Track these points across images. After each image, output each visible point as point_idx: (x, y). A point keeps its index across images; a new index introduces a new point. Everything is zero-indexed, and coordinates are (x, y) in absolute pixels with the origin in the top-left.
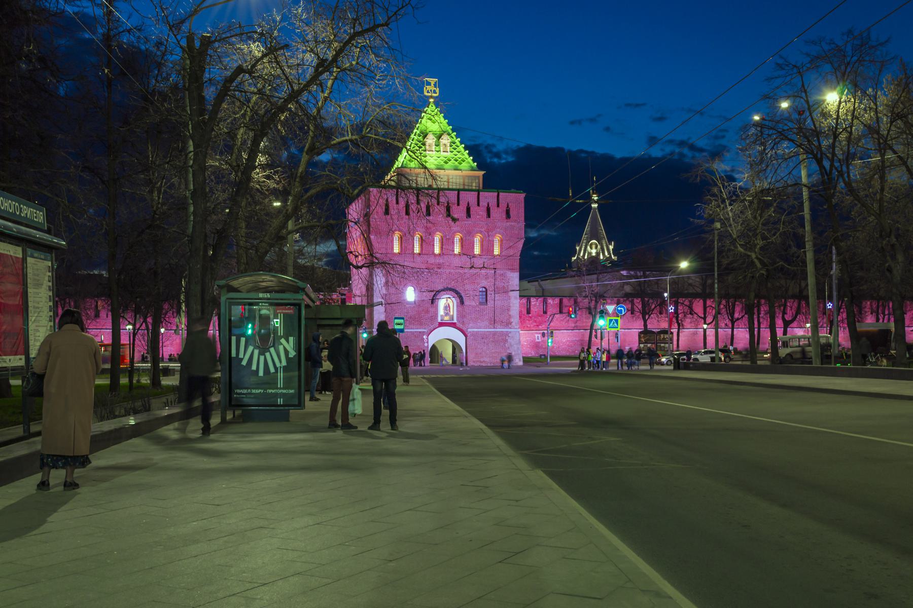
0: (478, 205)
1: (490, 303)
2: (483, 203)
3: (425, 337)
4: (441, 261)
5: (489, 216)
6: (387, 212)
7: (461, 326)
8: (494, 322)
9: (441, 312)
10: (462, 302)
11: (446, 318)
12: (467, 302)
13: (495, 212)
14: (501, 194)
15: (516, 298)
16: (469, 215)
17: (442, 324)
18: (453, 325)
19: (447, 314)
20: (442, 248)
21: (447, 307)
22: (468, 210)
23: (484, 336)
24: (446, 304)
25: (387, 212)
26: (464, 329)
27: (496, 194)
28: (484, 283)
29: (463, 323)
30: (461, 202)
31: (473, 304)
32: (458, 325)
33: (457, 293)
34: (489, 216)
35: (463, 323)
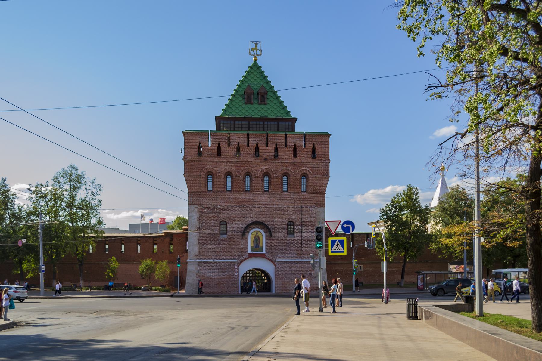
0: (286, 146)
1: (298, 236)
4: (251, 197)
5: (295, 155)
7: (270, 257)
8: (301, 253)
10: (270, 235)
16: (276, 156)
17: (251, 256)
18: (263, 256)
26: (273, 259)
28: (292, 217)
29: (272, 254)
30: (269, 144)
32: (267, 256)
34: (295, 155)
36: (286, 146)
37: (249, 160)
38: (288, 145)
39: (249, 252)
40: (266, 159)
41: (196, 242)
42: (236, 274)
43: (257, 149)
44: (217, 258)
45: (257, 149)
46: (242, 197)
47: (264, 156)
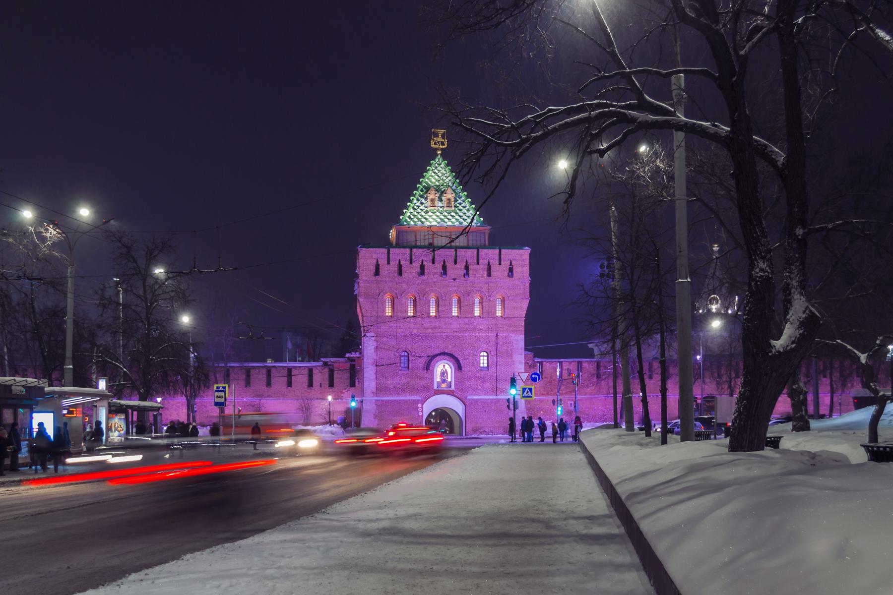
0: (478, 263)
1: (492, 369)
2: (484, 262)
3: (420, 405)
4: (437, 324)
5: (489, 274)
6: (377, 273)
7: (458, 394)
9: (438, 379)
10: (459, 367)
11: (444, 386)
12: (465, 368)
13: (495, 268)
14: (504, 252)
15: (520, 363)
18: (450, 393)
19: (444, 381)
20: (438, 311)
21: (444, 373)
22: (467, 267)
23: (485, 404)
24: (443, 369)
25: (377, 273)
27: (497, 251)
29: (462, 391)
30: (458, 261)
31: (473, 369)
33: (444, 354)
34: (489, 274)
35: (462, 391)
36: (478, 263)
37: (435, 280)
38: (480, 261)
39: (435, 388)
40: (454, 279)
41: (373, 376)
42: (420, 414)
43: (444, 267)
44: (397, 394)
45: (444, 267)
46: (427, 324)
47: (453, 276)
